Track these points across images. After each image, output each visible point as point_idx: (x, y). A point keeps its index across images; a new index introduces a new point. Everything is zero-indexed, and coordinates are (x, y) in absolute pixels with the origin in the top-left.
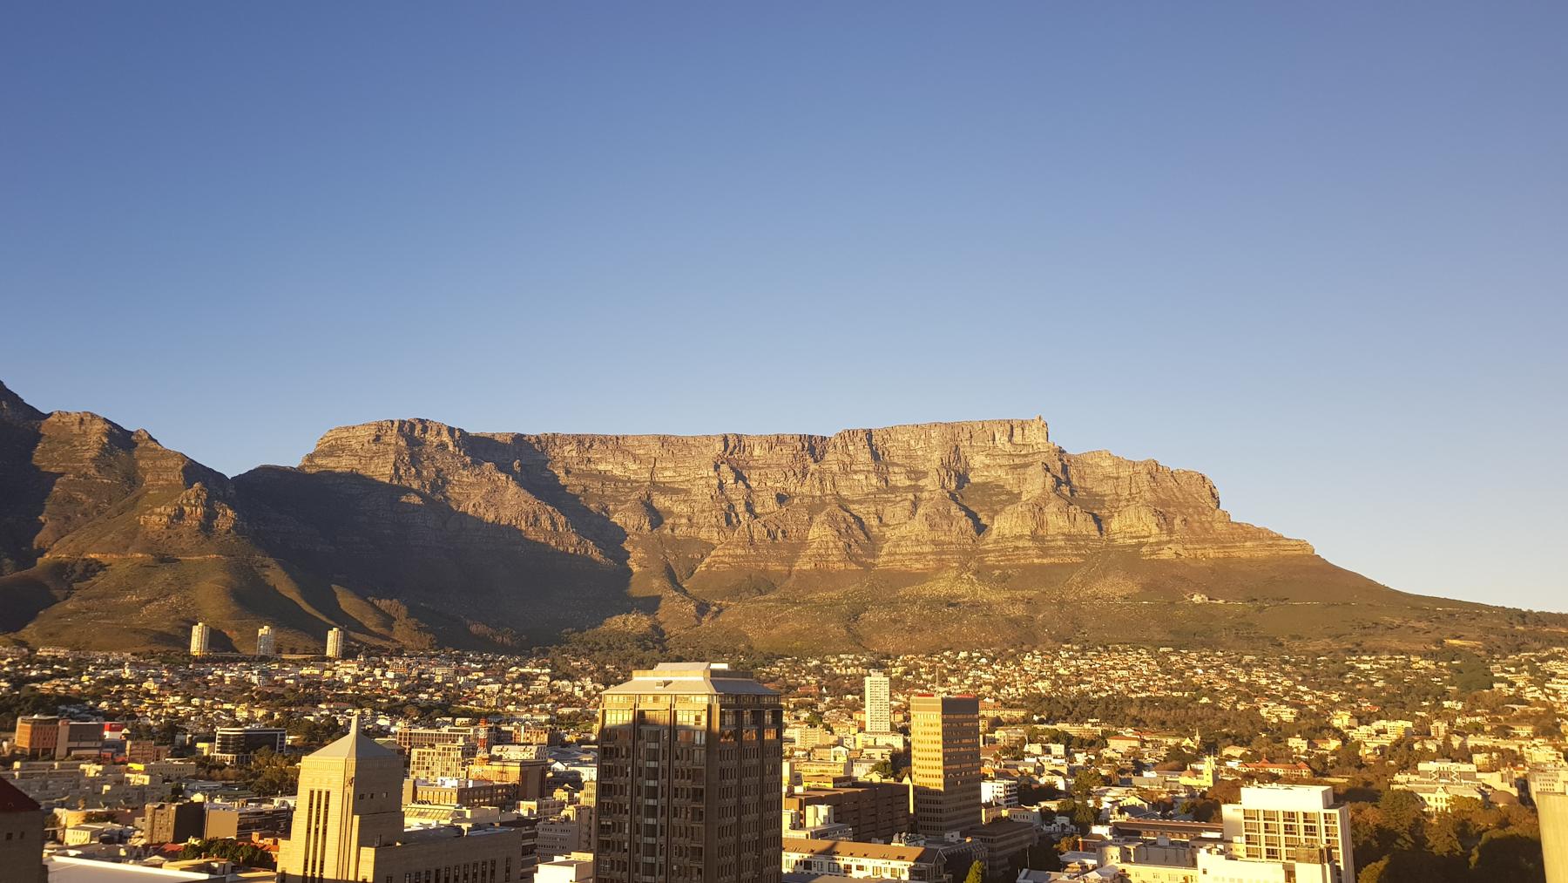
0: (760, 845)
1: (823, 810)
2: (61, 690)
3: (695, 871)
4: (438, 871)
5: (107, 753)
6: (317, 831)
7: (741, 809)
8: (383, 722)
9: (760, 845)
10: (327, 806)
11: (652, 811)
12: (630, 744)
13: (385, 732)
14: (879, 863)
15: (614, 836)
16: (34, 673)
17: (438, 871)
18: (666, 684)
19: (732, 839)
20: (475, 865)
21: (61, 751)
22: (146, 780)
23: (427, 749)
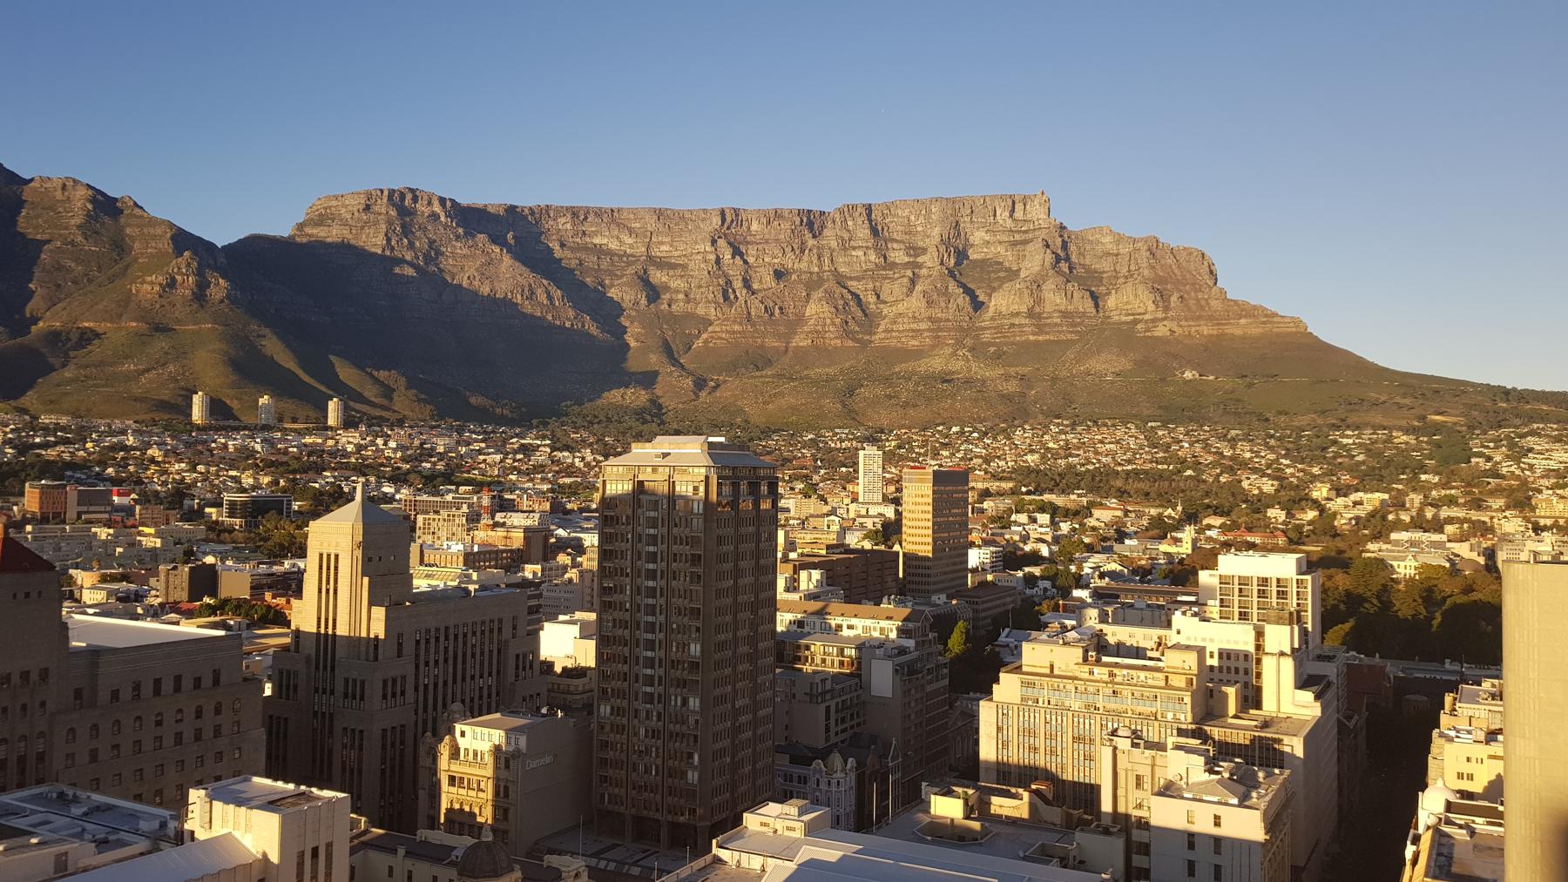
0: (754, 607)
1: (816, 574)
2: (66, 456)
4: (447, 628)
5: (117, 517)
6: (328, 591)
7: (737, 573)
8: (388, 489)
9: (754, 607)
10: (336, 568)
11: (652, 575)
12: (630, 512)
13: (389, 499)
14: (868, 622)
15: (615, 598)
16: (37, 440)
17: (447, 628)
18: (665, 455)
19: (729, 601)
20: (483, 623)
21: (71, 514)
22: (158, 543)
23: (432, 516)
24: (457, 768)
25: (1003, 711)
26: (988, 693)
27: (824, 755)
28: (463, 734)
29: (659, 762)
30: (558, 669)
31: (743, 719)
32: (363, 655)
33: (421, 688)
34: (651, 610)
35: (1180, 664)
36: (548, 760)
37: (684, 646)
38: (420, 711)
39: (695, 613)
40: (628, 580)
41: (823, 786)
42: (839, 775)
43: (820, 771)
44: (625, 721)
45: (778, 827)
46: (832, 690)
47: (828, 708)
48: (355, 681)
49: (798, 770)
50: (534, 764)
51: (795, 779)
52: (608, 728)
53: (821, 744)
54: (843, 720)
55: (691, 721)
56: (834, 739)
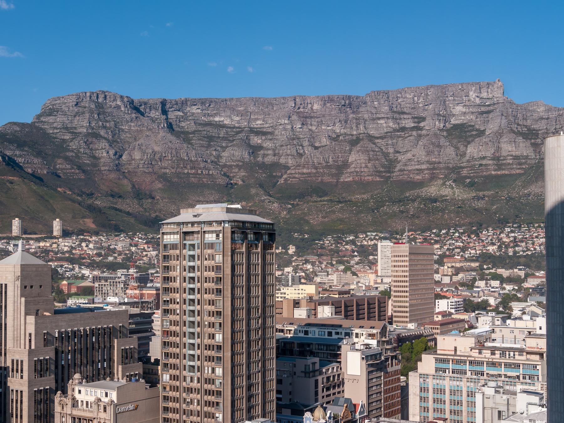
13: (83, 277)
15: (171, 306)
23: (103, 282)
24: (76, 413)
25: (424, 376)
26: (415, 369)
28: (80, 392)
30: (152, 361)
32: (22, 346)
33: (60, 367)
35: (535, 346)
37: (212, 336)
38: (60, 381)
39: (219, 313)
40: (178, 295)
44: (178, 383)
47: (317, 381)
48: (17, 361)
52: (168, 389)
54: (328, 389)
55: (217, 382)
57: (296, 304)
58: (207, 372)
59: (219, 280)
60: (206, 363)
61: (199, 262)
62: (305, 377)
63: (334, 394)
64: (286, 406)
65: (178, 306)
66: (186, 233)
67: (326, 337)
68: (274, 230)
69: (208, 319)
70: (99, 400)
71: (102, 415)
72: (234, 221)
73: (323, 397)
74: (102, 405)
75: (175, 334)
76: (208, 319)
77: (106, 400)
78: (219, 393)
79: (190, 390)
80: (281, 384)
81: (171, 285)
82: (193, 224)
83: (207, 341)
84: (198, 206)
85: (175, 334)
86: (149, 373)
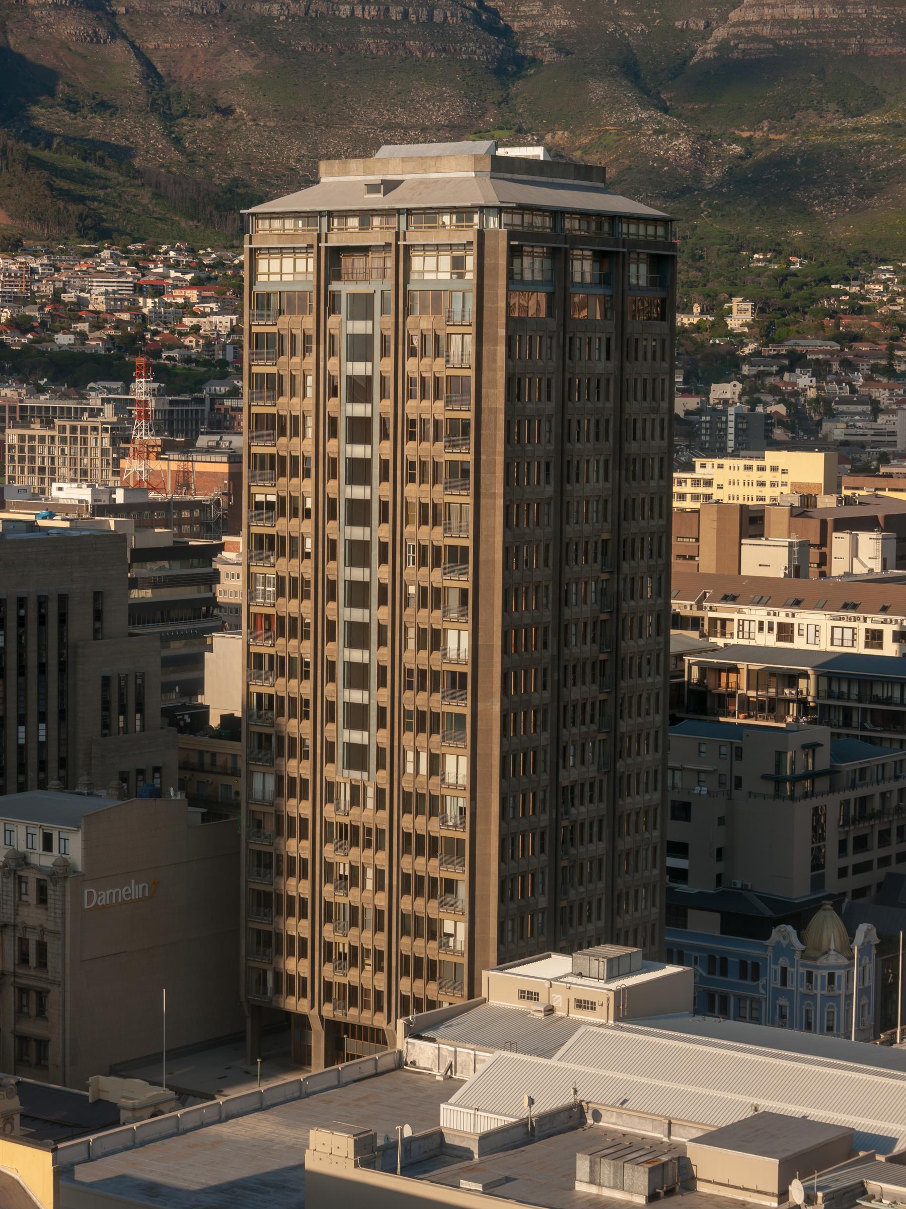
0: (615, 552)
3: (454, 599)
9: (615, 552)
11: (359, 471)
15: (283, 526)
18: (390, 186)
20: (22, 602)
23: (36, 430)
27: (800, 917)
29: (381, 900)
30: (214, 721)
31: (582, 811)
34: (359, 553)
36: (136, 890)
37: (434, 640)
40: (308, 485)
41: (796, 985)
42: (833, 959)
43: (789, 951)
45: (558, 1001)
46: (831, 773)
49: (742, 948)
50: (103, 898)
51: (733, 961)
53: (799, 889)
54: (861, 843)
56: (833, 884)
57: (752, 522)
58: (415, 768)
59: (458, 431)
60: (408, 738)
61: (386, 365)
62: (778, 795)
63: (884, 861)
64: (703, 902)
65: (307, 526)
66: (336, 254)
67: (861, 649)
68: (673, 246)
69: (416, 577)
70: (22, 860)
71: (32, 915)
72: (522, 209)
73: (842, 873)
74: (32, 877)
75: (292, 627)
76: (416, 577)
77: (46, 861)
78: (454, 848)
79: (350, 835)
80: (687, 819)
81: (285, 446)
82: (365, 216)
83: (414, 657)
84: (385, 151)
85: (292, 627)
86: (201, 768)
